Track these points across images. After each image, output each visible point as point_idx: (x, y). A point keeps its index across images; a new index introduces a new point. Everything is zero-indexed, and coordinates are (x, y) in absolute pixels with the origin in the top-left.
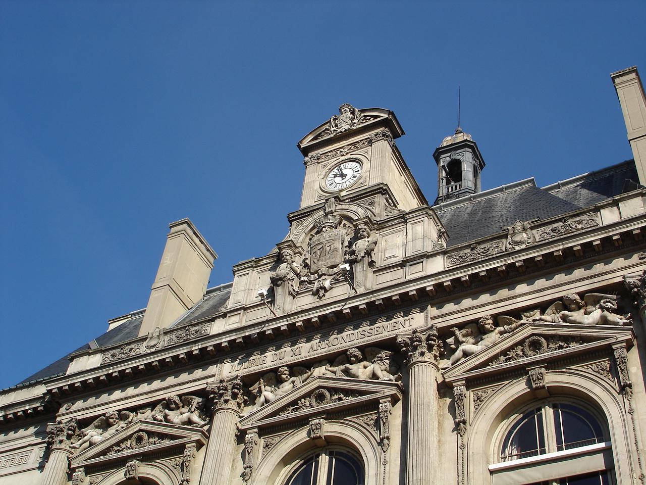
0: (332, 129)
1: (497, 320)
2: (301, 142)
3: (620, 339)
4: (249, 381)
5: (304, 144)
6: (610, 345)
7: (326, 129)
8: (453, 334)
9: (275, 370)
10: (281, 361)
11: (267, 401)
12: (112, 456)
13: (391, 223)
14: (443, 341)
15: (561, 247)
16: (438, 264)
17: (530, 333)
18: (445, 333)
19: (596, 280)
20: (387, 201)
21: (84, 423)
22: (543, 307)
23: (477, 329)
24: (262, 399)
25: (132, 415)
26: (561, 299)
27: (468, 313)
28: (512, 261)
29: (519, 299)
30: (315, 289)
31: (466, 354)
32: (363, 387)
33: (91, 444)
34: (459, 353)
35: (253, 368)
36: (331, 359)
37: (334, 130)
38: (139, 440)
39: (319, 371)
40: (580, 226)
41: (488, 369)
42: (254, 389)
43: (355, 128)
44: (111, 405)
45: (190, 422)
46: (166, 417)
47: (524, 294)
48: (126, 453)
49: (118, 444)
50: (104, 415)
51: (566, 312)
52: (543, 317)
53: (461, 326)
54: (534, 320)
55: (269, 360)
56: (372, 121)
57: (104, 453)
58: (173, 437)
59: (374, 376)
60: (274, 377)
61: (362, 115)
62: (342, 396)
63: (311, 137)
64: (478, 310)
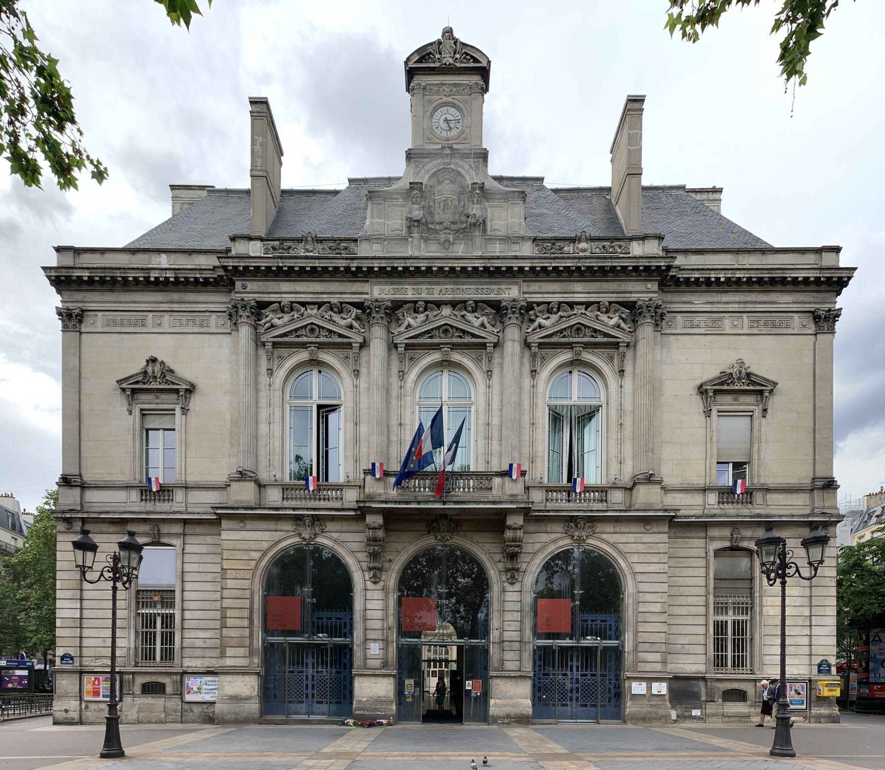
4: (397, 305)
6: (618, 343)
7: (430, 53)
8: (533, 309)
9: (415, 302)
11: (409, 326)
12: (290, 339)
18: (530, 307)
23: (550, 309)
25: (303, 309)
29: (576, 295)
31: (540, 326)
33: (272, 326)
34: (536, 324)
35: (398, 296)
36: (454, 304)
38: (312, 330)
39: (446, 311)
40: (619, 250)
41: (554, 339)
42: (399, 313)
43: (458, 65)
45: (351, 327)
47: (580, 291)
48: (305, 339)
50: (280, 303)
51: (599, 313)
53: (539, 304)
55: (409, 291)
57: (285, 335)
59: (483, 325)
60: (415, 307)
61: (464, 51)
64: (551, 295)
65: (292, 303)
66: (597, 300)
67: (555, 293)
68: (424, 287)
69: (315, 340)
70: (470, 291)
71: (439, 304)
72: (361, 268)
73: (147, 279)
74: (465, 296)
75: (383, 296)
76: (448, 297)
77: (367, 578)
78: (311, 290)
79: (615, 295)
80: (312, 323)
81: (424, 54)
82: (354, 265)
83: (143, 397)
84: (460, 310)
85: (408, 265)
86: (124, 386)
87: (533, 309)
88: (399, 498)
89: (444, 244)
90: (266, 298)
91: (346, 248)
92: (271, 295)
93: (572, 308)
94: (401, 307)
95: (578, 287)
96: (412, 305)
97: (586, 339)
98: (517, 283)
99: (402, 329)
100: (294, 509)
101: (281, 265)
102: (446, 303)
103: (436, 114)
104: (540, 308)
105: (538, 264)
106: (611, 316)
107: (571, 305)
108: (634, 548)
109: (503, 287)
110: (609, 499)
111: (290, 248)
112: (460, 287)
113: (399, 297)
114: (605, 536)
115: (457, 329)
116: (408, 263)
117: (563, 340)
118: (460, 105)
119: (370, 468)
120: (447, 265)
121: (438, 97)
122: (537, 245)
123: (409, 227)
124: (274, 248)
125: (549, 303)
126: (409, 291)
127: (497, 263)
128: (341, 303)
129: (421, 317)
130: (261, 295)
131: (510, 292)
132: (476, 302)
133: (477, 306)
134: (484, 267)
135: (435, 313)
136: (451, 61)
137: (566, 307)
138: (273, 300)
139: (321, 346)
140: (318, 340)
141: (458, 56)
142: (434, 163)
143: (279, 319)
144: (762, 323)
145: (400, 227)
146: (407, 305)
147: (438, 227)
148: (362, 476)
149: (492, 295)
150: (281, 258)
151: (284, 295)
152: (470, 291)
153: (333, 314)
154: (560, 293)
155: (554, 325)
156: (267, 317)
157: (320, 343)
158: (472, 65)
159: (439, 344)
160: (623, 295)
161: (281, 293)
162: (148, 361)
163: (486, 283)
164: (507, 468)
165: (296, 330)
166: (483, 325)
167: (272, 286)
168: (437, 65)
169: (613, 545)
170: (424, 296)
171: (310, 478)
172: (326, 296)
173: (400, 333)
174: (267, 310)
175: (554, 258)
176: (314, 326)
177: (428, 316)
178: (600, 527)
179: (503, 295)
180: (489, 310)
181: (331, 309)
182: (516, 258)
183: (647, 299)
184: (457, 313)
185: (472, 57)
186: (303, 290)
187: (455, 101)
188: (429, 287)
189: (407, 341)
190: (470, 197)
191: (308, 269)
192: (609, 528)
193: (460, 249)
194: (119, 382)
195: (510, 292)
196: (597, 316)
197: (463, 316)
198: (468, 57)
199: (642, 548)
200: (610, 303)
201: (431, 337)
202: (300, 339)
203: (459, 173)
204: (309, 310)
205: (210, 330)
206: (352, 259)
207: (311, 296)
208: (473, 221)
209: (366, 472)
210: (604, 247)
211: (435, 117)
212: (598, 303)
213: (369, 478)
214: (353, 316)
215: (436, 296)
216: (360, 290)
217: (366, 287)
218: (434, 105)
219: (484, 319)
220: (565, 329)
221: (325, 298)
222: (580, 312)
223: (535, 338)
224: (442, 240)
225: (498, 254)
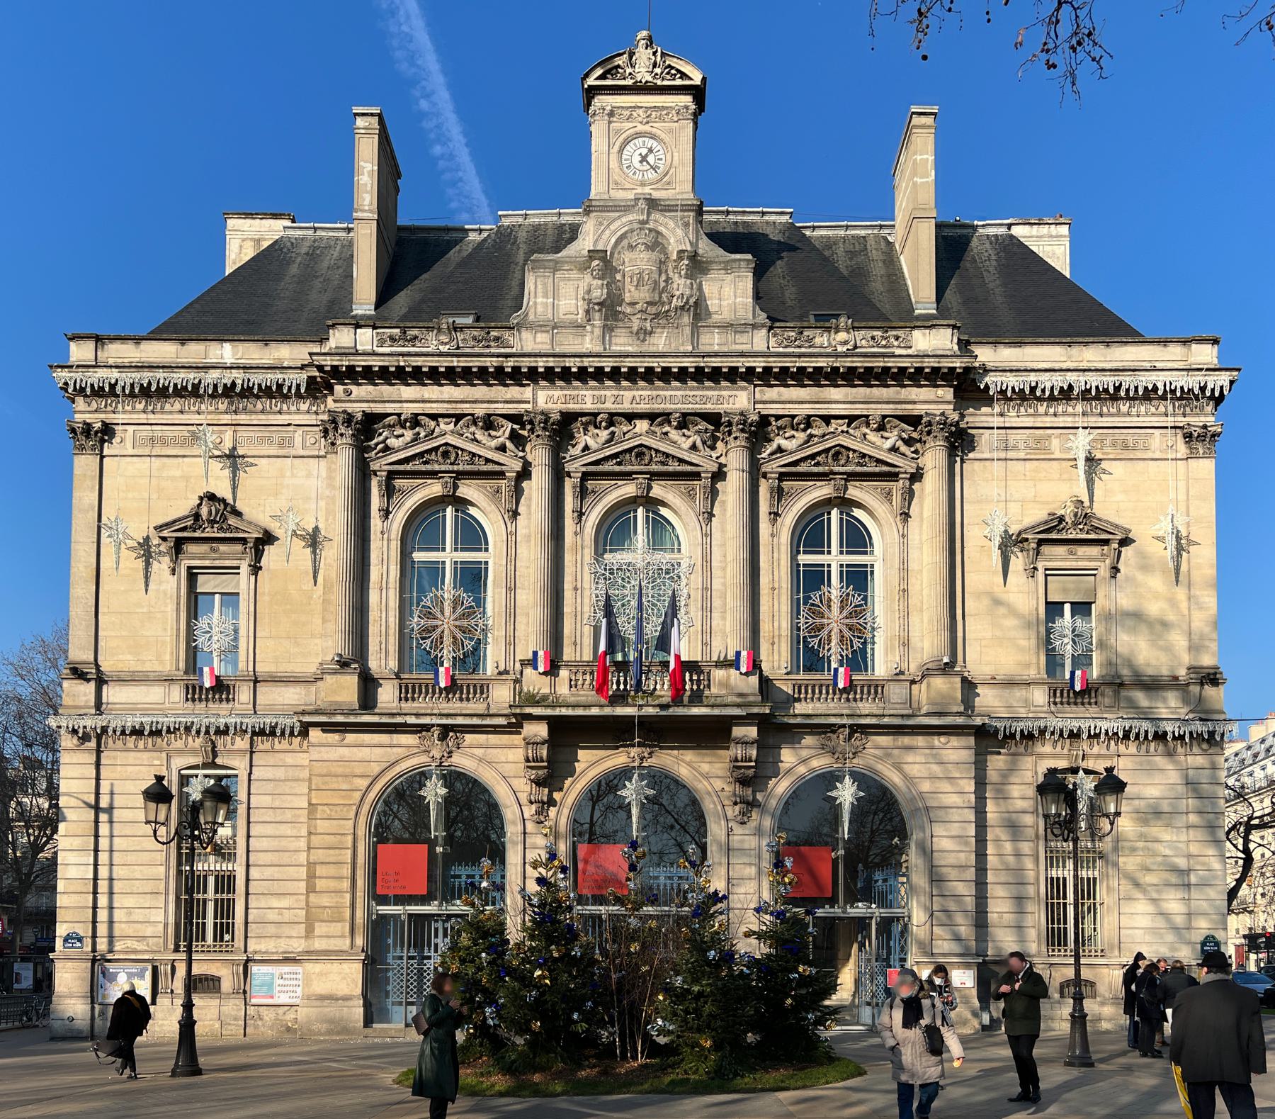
2: (587, 75)
4: (569, 418)
5: (591, 81)
7: (619, 66)
9: (596, 415)
11: (586, 448)
19: (899, 406)
22: (851, 419)
25: (433, 424)
29: (834, 406)
31: (780, 450)
36: (651, 417)
40: (896, 343)
41: (802, 468)
43: (659, 82)
45: (502, 448)
48: (436, 467)
50: (399, 415)
51: (868, 431)
53: (778, 417)
55: (587, 398)
63: (599, 72)
64: (796, 406)
65: (417, 415)
66: (865, 413)
67: (802, 402)
69: (451, 468)
70: (677, 398)
71: (631, 417)
72: (520, 368)
74: (669, 407)
75: (550, 406)
76: (643, 407)
78: (446, 397)
79: (891, 406)
80: (446, 444)
82: (509, 364)
83: (191, 548)
84: (660, 424)
85: (586, 364)
86: (165, 533)
88: (572, 700)
89: (637, 333)
90: (379, 408)
91: (497, 339)
92: (387, 405)
93: (828, 424)
97: (848, 469)
99: (577, 451)
100: (417, 715)
101: (402, 364)
102: (641, 416)
103: (628, 148)
104: (780, 423)
105: (776, 363)
106: (886, 434)
107: (827, 419)
111: (416, 337)
113: (572, 407)
115: (657, 451)
116: (586, 362)
117: (816, 469)
118: (663, 136)
119: (530, 656)
120: (641, 364)
121: (631, 125)
122: (775, 335)
123: (587, 312)
124: (392, 339)
125: (793, 417)
126: (587, 398)
127: (716, 362)
130: (372, 405)
131: (736, 400)
132: (684, 415)
134: (696, 368)
135: (625, 429)
136: (650, 79)
137: (819, 422)
139: (461, 475)
140: (456, 468)
141: (658, 70)
142: (624, 220)
143: (398, 437)
144: (1108, 443)
145: (573, 310)
147: (628, 310)
148: (518, 665)
149: (709, 406)
150: (403, 354)
151: (405, 405)
152: (677, 398)
155: (801, 447)
156: (380, 434)
158: (678, 82)
159: (630, 474)
161: (401, 402)
162: (201, 499)
164: (731, 656)
165: (421, 455)
166: (694, 447)
167: (386, 390)
168: (629, 82)
170: (610, 406)
171: (442, 670)
172: (468, 405)
173: (574, 458)
174: (380, 425)
175: (799, 356)
176: (450, 449)
177: (613, 433)
179: (725, 406)
180: (703, 425)
181: (475, 423)
182: (743, 355)
183: (938, 412)
184: (657, 429)
185: (678, 71)
186: (434, 397)
187: (654, 130)
188: (616, 393)
189: (584, 469)
190: (676, 267)
191: (442, 369)
193: (660, 341)
195: (736, 400)
196: (865, 435)
197: (666, 434)
198: (673, 72)
201: (619, 464)
202: (429, 467)
203: (658, 233)
204: (442, 426)
205: (294, 453)
206: (507, 356)
207: (446, 405)
208: (680, 304)
209: (524, 663)
210: (873, 338)
211: (625, 152)
212: (867, 416)
213: (529, 671)
214: (507, 434)
215: (626, 407)
216: (518, 397)
217: (527, 392)
218: (624, 136)
220: (819, 453)
221: (466, 408)
222: (840, 429)
223: (773, 467)
224: (635, 329)
225: (716, 348)
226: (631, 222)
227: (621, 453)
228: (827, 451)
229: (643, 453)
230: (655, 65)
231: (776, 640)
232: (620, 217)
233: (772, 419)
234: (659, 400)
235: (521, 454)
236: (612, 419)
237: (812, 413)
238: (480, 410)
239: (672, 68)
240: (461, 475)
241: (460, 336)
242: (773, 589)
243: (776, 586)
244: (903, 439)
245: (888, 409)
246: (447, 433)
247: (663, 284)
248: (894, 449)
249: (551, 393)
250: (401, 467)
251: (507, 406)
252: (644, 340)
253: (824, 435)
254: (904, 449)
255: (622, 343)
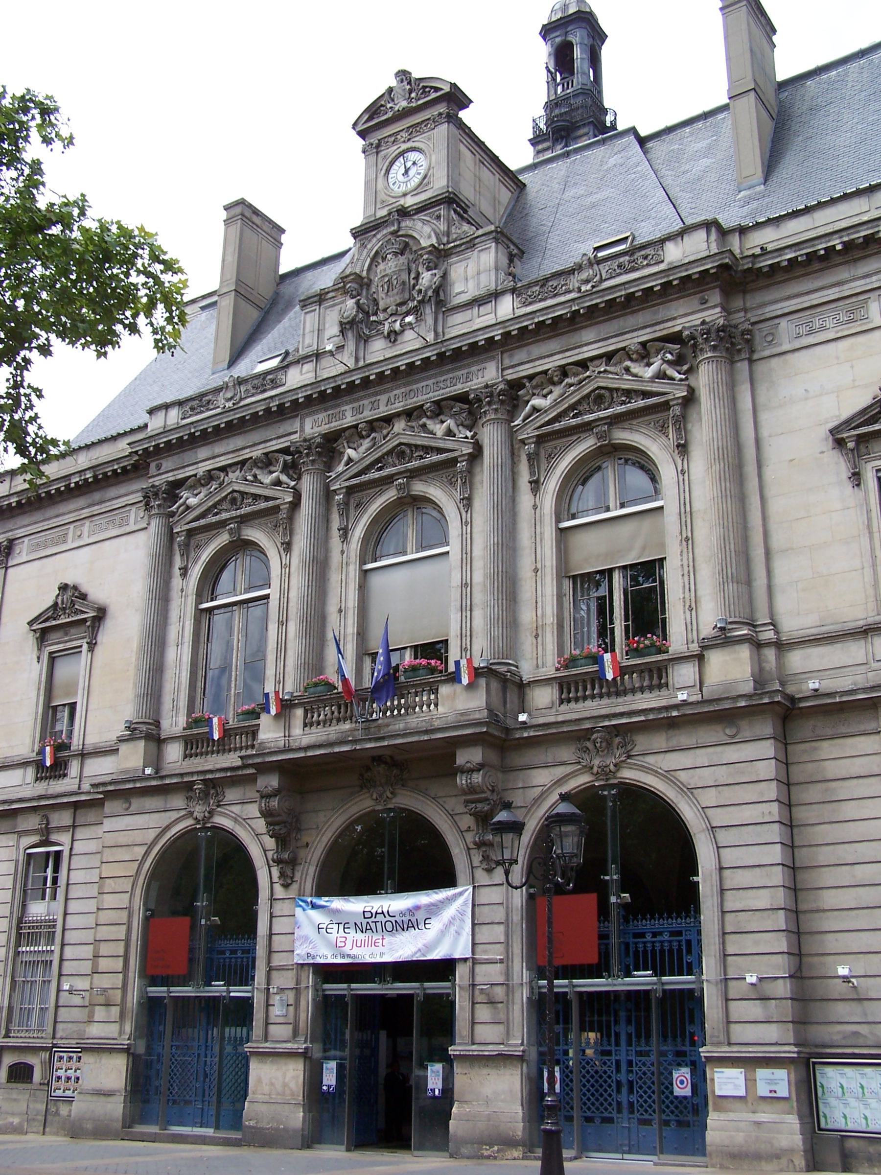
0: (389, 106)
1: (564, 371)
3: (677, 396)
6: (667, 403)
7: (382, 106)
9: (356, 426)
10: (361, 416)
11: (350, 460)
13: (458, 250)
14: (512, 395)
15: (623, 293)
16: (506, 307)
17: (596, 386)
19: (657, 328)
20: (455, 211)
21: (178, 484)
22: (609, 357)
23: (544, 381)
24: (346, 458)
25: (222, 475)
26: (624, 349)
27: (537, 363)
28: (577, 308)
29: (585, 349)
30: (386, 333)
31: (535, 409)
32: (441, 444)
33: (188, 508)
35: (333, 425)
36: (408, 414)
37: (391, 108)
38: (233, 501)
41: (557, 426)
43: (414, 105)
44: (200, 465)
46: (255, 476)
48: (224, 516)
49: (215, 506)
50: (195, 475)
52: (608, 368)
53: (531, 378)
54: (600, 372)
55: (348, 416)
56: (434, 95)
57: (203, 515)
58: (267, 499)
60: (354, 433)
61: (421, 85)
62: (421, 453)
64: (547, 360)
65: (209, 471)
67: (552, 355)
68: (366, 402)
71: (388, 420)
73: (67, 486)
77: (476, 863)
78: (231, 447)
81: (374, 110)
83: (54, 637)
86: (35, 627)
87: (524, 386)
94: (340, 436)
95: (588, 335)
96: (353, 430)
98: (493, 358)
102: (398, 415)
104: (534, 382)
107: (583, 364)
108: (706, 776)
109: (474, 369)
110: (671, 683)
112: (414, 387)
113: (335, 425)
114: (651, 759)
125: (545, 372)
128: (266, 454)
129: (366, 443)
132: (437, 403)
133: (439, 409)
135: (385, 432)
137: (575, 369)
138: (188, 474)
139: (244, 520)
146: (347, 433)
153: (258, 472)
154: (559, 353)
155: (556, 404)
156: (181, 497)
157: (241, 516)
160: (662, 326)
162: (59, 589)
163: (448, 372)
166: (449, 433)
168: (390, 114)
169: (667, 776)
178: (642, 742)
184: (414, 424)
185: (432, 87)
189: (347, 484)
192: (659, 741)
194: (30, 623)
198: (427, 89)
199: (722, 775)
200: (644, 344)
204: (230, 474)
215: (384, 410)
219: (450, 422)
221: (246, 454)
223: (529, 433)
226: (385, 236)
227: (382, 457)
228: (588, 396)
229: (403, 452)
230: (410, 92)
231: (540, 632)
232: (374, 235)
233: (525, 381)
234: (412, 394)
235: (293, 483)
236: (373, 425)
237: (563, 362)
238: (257, 453)
239: (427, 87)
240: (244, 520)
241: (243, 388)
242: (536, 570)
243: (539, 566)
244: (669, 362)
245: (645, 335)
246: (235, 481)
247: (412, 282)
248: (661, 375)
249: (316, 417)
250: (202, 522)
251: (280, 441)
252: (395, 340)
253: (580, 382)
254: (671, 372)
255: (378, 350)
